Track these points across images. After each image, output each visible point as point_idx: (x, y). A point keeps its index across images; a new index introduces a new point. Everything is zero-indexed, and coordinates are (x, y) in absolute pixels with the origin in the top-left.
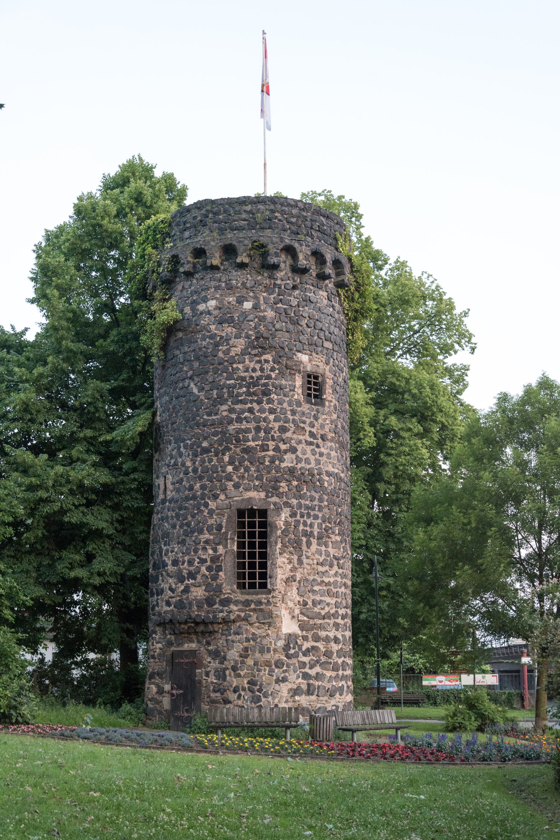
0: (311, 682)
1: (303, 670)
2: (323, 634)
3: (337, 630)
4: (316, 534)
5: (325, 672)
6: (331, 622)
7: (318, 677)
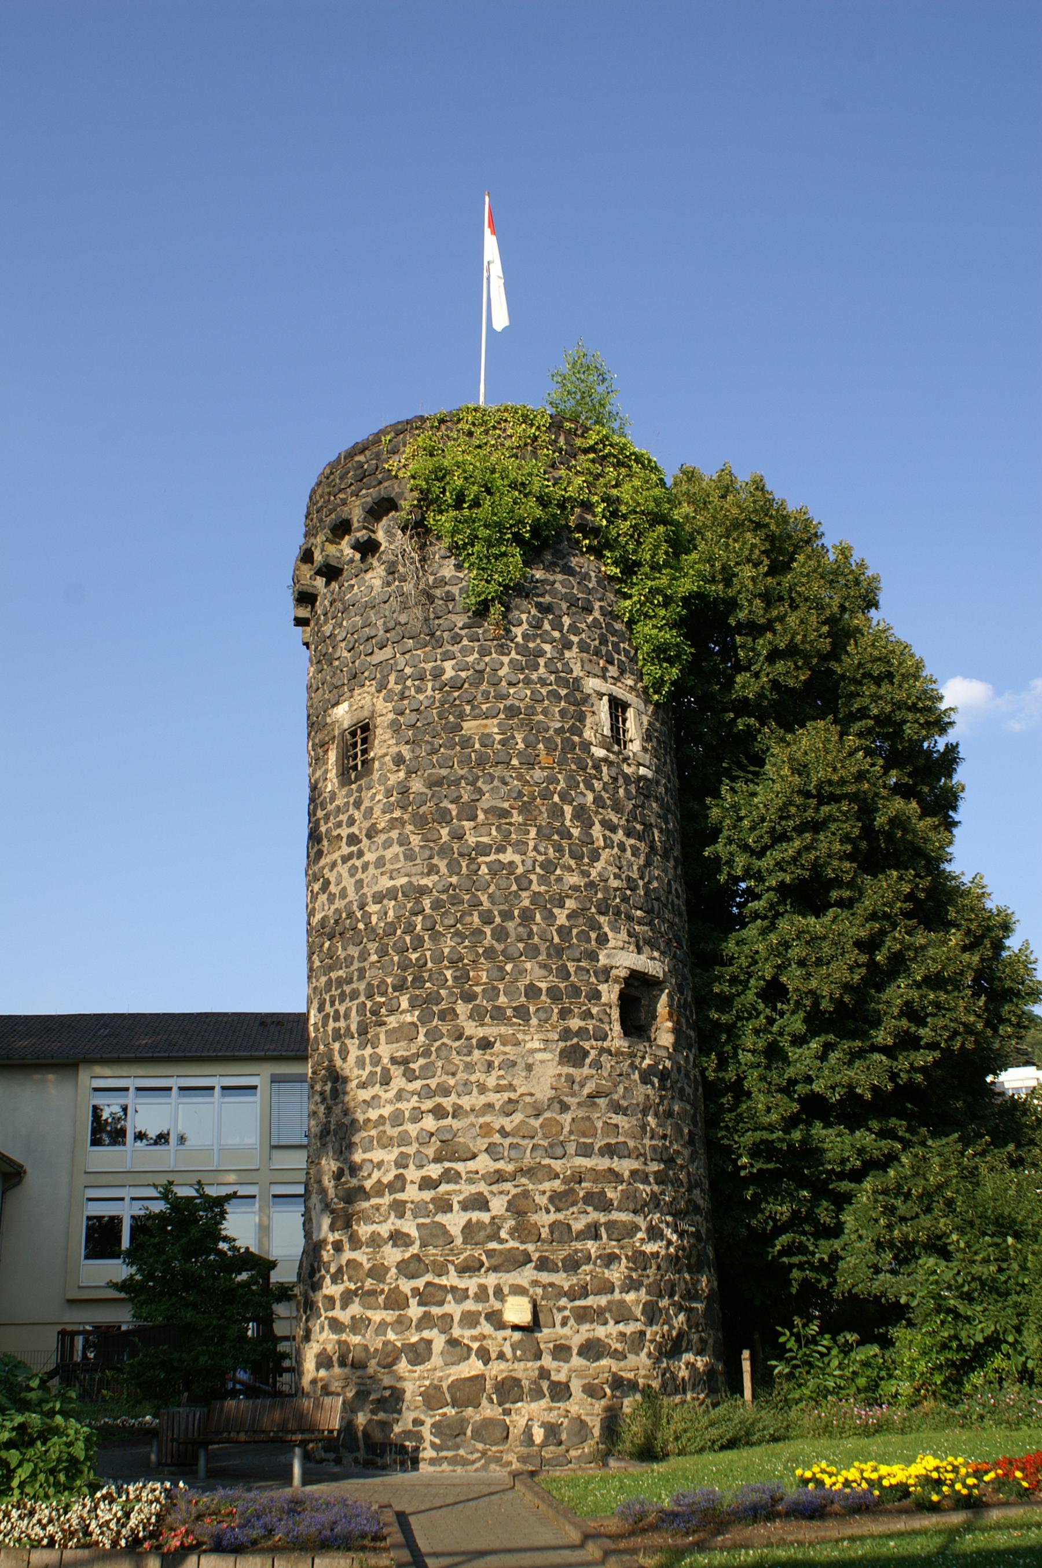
0: (344, 1337)
1: (330, 1314)
3: (401, 1216)
4: (354, 1028)
5: (369, 1313)
6: (387, 1199)
7: (358, 1325)
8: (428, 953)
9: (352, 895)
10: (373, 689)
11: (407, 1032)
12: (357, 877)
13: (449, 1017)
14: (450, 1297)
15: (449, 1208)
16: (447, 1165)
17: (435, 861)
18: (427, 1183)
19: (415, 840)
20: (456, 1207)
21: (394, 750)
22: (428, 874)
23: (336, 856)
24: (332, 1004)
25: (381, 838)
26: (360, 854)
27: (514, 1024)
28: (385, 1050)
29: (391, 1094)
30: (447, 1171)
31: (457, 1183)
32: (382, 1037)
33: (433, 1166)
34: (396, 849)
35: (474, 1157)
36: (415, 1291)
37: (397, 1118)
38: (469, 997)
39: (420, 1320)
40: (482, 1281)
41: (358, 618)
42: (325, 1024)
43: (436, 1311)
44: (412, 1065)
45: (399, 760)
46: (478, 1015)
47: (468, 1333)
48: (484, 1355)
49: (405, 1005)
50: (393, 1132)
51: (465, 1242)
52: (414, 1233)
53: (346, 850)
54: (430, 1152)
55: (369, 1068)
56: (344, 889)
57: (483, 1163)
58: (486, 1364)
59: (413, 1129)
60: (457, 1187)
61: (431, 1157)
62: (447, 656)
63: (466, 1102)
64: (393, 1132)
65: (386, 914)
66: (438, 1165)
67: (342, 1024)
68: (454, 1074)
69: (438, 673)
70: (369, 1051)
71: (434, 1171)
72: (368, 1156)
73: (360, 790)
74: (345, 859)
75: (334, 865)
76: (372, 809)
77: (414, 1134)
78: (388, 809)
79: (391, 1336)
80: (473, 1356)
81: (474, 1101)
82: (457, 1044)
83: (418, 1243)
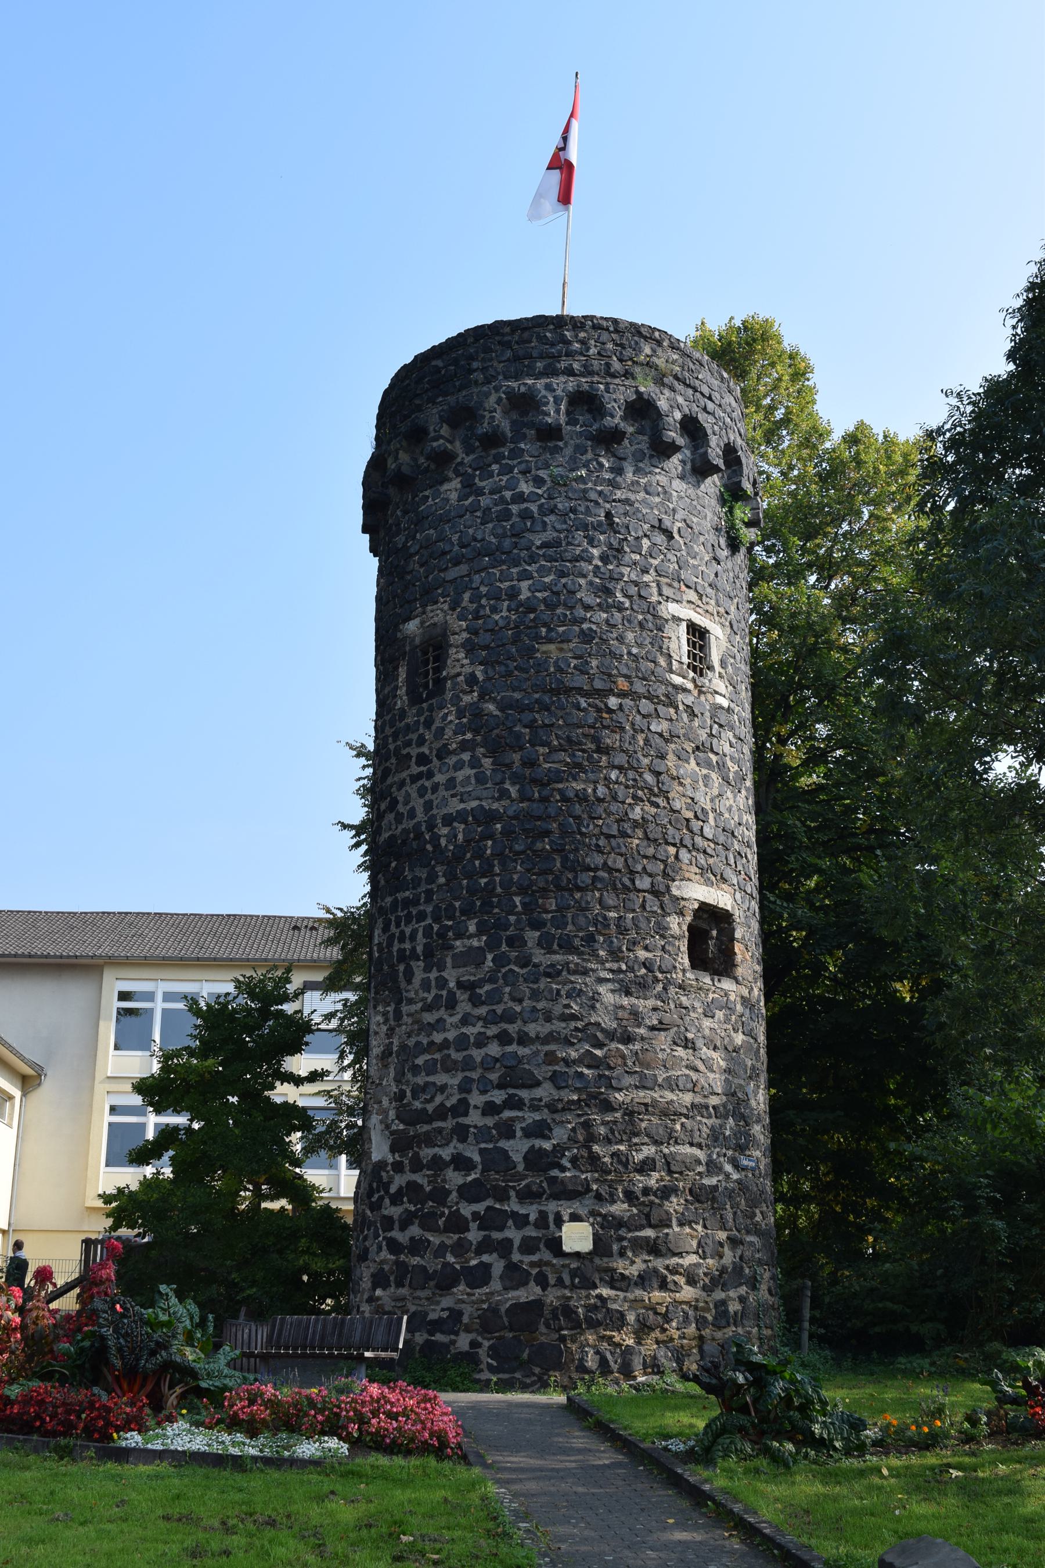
2: (427, 1153)
3: (463, 1139)
4: (419, 949)
6: (448, 1124)
7: (417, 1246)
8: (497, 879)
9: (420, 816)
10: (446, 607)
11: (474, 957)
12: (427, 798)
13: (517, 944)
14: (510, 1223)
15: (510, 1135)
16: (511, 1091)
17: (507, 786)
18: (490, 1109)
19: (487, 762)
20: (519, 1133)
21: (468, 670)
22: (499, 799)
23: (404, 774)
24: (398, 925)
25: (452, 760)
26: (430, 775)
27: (583, 953)
28: (451, 976)
29: (455, 1019)
30: (511, 1096)
31: (520, 1109)
32: (449, 960)
33: (496, 1092)
34: (468, 771)
35: (538, 1084)
36: (475, 1215)
37: (462, 1043)
38: (536, 925)
39: (480, 1244)
40: (543, 1208)
41: (432, 531)
42: (390, 945)
43: (496, 1235)
44: (478, 991)
45: (472, 680)
46: (546, 944)
47: (528, 1259)
48: (542, 1281)
49: (472, 929)
50: (456, 1056)
51: (526, 1169)
52: (477, 1158)
53: (415, 770)
54: (494, 1077)
55: (434, 992)
56: (413, 809)
58: (544, 1289)
59: (477, 1054)
60: (520, 1114)
61: (496, 1082)
62: (525, 576)
63: (532, 1029)
64: (456, 1056)
65: (455, 836)
66: (502, 1092)
67: (407, 946)
68: (520, 1001)
69: (513, 594)
70: (433, 975)
71: (498, 1097)
72: (431, 1079)
73: (431, 709)
74: (414, 779)
75: (402, 784)
76: (443, 729)
77: (479, 1059)
78: (460, 730)
79: (450, 1259)
80: (532, 1283)
81: (539, 1029)
82: (525, 971)
83: (480, 1167)
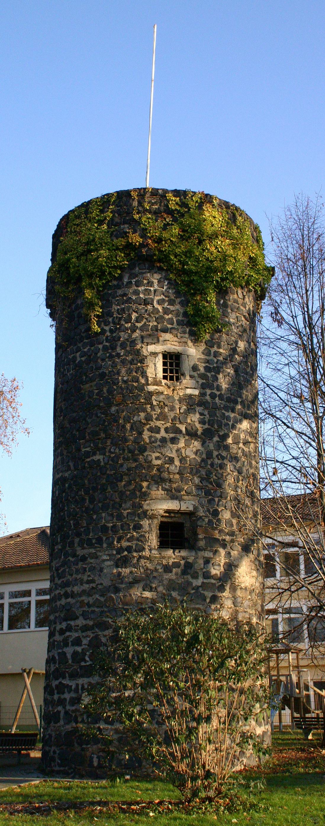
15: (66, 645)
27: (96, 547)
35: (77, 618)
38: (78, 535)
40: (77, 682)
51: (72, 662)
57: (81, 622)
62: (78, 350)
68: (72, 575)
